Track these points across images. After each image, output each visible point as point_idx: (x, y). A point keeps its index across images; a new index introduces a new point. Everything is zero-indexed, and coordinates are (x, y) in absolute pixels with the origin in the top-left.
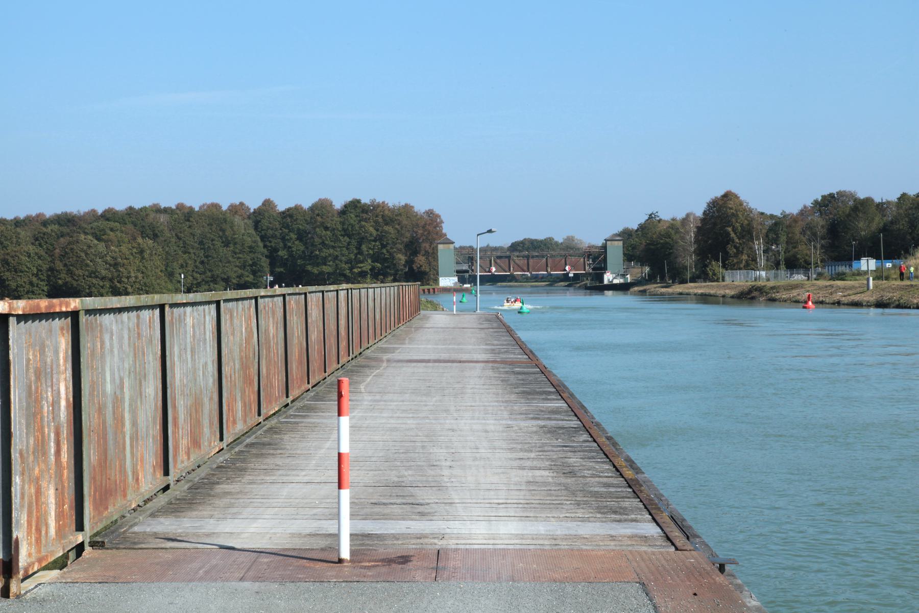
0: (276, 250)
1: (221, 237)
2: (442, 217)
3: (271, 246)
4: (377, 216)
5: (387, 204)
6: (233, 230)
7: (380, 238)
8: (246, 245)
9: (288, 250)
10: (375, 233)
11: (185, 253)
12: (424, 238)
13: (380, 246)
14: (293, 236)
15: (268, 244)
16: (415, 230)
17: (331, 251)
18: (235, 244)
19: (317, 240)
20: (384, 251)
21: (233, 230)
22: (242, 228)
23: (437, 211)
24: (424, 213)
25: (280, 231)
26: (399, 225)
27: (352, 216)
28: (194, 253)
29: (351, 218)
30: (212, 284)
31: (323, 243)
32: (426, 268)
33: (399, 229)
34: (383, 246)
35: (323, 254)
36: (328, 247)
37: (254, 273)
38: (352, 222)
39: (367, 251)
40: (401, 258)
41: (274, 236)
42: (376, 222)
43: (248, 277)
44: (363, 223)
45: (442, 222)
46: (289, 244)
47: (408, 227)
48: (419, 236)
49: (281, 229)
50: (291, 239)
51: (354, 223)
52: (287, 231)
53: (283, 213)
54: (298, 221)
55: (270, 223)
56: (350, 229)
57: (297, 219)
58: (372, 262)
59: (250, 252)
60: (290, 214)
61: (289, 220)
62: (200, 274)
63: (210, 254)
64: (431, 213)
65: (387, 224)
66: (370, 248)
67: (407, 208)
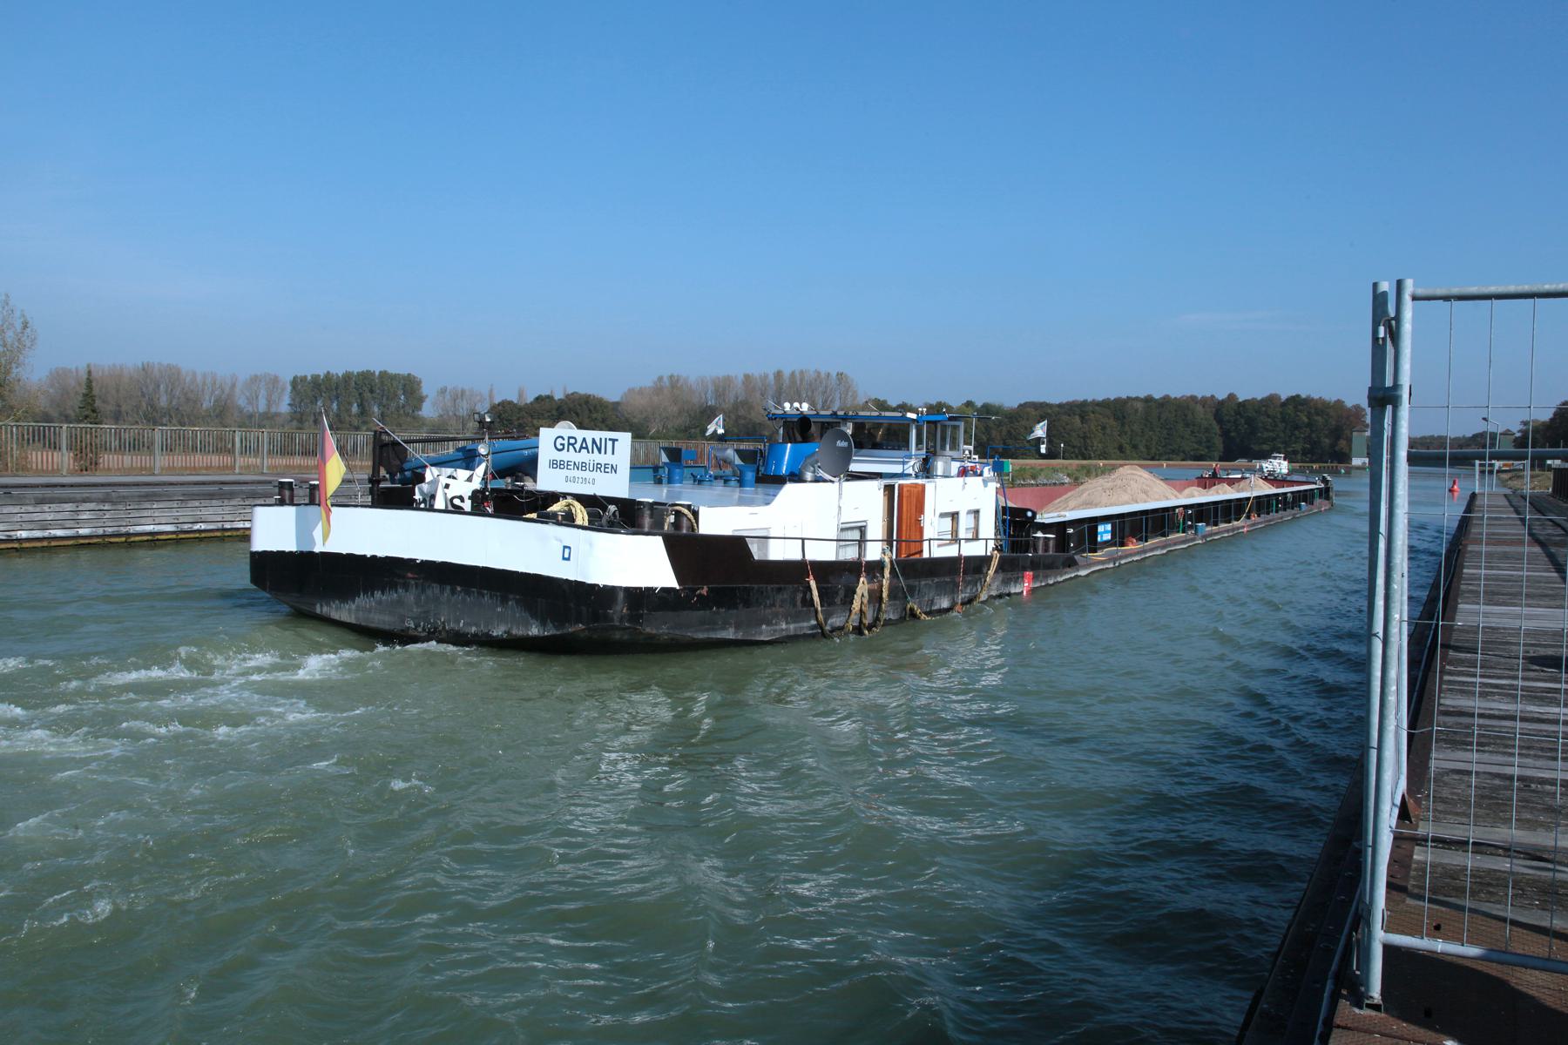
0: (1229, 431)
7: (1309, 425)
10: (1306, 420)
14: (1243, 421)
15: (1224, 427)
17: (1271, 434)
19: (1260, 425)
20: (1314, 435)
22: (1202, 416)
27: (1291, 407)
32: (1346, 450)
34: (1312, 431)
35: (1265, 436)
36: (1267, 430)
37: (1208, 447)
41: (1229, 421)
42: (1309, 413)
44: (1299, 413)
46: (1240, 427)
60: (1244, 404)
65: (1318, 414)
67: (1339, 403)
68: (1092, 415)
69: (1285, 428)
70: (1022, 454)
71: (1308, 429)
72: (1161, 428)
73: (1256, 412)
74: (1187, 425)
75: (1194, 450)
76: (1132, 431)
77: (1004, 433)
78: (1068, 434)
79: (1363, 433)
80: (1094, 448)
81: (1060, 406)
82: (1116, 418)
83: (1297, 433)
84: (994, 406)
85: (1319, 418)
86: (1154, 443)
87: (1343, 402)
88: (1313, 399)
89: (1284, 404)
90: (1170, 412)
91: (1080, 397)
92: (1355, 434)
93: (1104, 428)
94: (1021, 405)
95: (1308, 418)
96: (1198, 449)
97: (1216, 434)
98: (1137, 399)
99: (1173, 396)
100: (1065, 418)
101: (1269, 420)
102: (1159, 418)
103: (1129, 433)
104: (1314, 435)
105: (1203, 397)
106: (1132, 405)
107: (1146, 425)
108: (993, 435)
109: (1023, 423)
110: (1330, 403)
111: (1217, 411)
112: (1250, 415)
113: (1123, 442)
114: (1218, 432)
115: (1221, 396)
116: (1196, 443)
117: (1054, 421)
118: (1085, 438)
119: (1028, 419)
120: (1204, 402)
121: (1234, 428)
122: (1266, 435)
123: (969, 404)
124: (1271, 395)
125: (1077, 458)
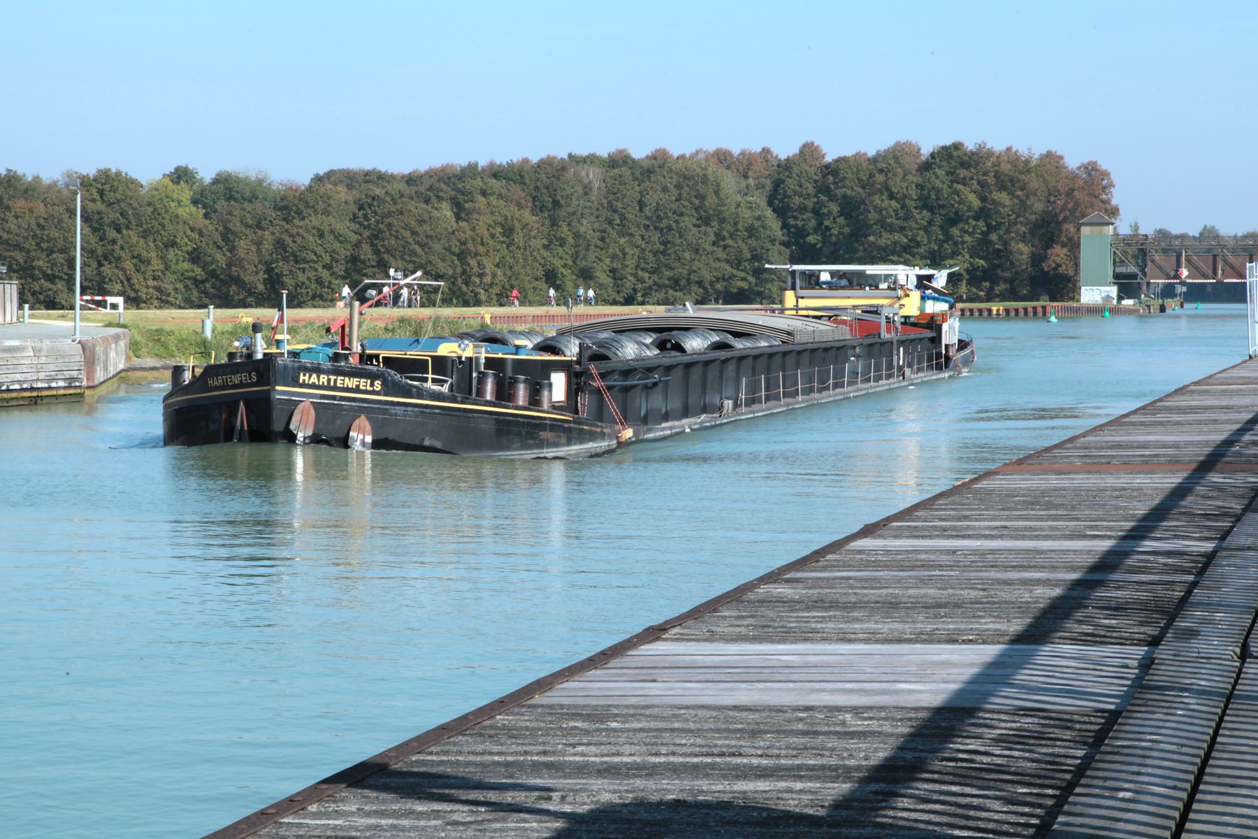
1: (697, 209)
2: (1112, 176)
3: (796, 226)
4: (985, 174)
5: (1017, 151)
6: (719, 199)
7: (981, 214)
8: (740, 226)
9: (823, 235)
10: (976, 203)
11: (622, 234)
12: (1068, 214)
13: (985, 229)
14: (834, 208)
15: (791, 221)
16: (1052, 199)
17: (897, 236)
18: (722, 221)
19: (873, 216)
20: (994, 237)
21: (719, 199)
23: (1103, 165)
24: (1079, 168)
25: (815, 200)
26: (1022, 189)
27: (941, 172)
28: (642, 236)
29: (937, 177)
30: (671, 292)
31: (882, 223)
33: (1024, 198)
34: (991, 229)
35: (882, 242)
36: (890, 228)
38: (938, 183)
39: (961, 236)
40: (1023, 251)
41: (802, 209)
43: (743, 279)
44: (955, 185)
45: (1111, 185)
46: (827, 223)
47: (1039, 194)
48: (1058, 211)
49: (816, 196)
50: (830, 213)
51: (941, 185)
52: (826, 198)
53: (827, 166)
54: (847, 182)
55: (800, 186)
56: (933, 196)
57: (845, 178)
58: (971, 257)
59: (750, 237)
60: (833, 170)
61: (831, 178)
62: (650, 273)
63: (670, 238)
64: (1092, 169)
65: (1002, 188)
66: (967, 232)
67: (1051, 160)
68: (481, 199)
69: (931, 222)
70: (313, 298)
71: (981, 223)
72: (646, 227)
73: (863, 187)
74: (706, 221)
75: (724, 279)
76: (577, 236)
77: (267, 246)
78: (422, 246)
79: (1105, 228)
80: (488, 279)
81: (411, 180)
82: (538, 208)
83: (955, 231)
84: (246, 182)
85: (1003, 197)
86: (631, 263)
87: (1061, 158)
88: (990, 154)
89: (926, 167)
90: (665, 190)
91: (460, 159)
92: (1085, 230)
93: (508, 232)
94: (318, 179)
95: (983, 199)
96: (732, 277)
97: (773, 241)
98: (591, 160)
99: (675, 153)
100: (415, 207)
101: (893, 203)
102: (641, 204)
103: (571, 240)
104: (994, 237)
105: (743, 153)
106: (576, 174)
107: (610, 222)
108: (241, 253)
109: (315, 221)
110: (1027, 162)
111: (778, 184)
112: (849, 192)
113: (557, 263)
114: (779, 234)
115: (785, 149)
116: (727, 261)
117: (390, 214)
118: (462, 256)
119: (326, 212)
120: (743, 165)
121: (813, 223)
122: (886, 239)
123: (181, 175)
124: (898, 144)
125: (447, 302)
